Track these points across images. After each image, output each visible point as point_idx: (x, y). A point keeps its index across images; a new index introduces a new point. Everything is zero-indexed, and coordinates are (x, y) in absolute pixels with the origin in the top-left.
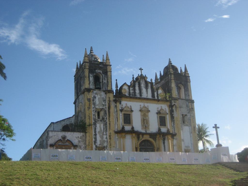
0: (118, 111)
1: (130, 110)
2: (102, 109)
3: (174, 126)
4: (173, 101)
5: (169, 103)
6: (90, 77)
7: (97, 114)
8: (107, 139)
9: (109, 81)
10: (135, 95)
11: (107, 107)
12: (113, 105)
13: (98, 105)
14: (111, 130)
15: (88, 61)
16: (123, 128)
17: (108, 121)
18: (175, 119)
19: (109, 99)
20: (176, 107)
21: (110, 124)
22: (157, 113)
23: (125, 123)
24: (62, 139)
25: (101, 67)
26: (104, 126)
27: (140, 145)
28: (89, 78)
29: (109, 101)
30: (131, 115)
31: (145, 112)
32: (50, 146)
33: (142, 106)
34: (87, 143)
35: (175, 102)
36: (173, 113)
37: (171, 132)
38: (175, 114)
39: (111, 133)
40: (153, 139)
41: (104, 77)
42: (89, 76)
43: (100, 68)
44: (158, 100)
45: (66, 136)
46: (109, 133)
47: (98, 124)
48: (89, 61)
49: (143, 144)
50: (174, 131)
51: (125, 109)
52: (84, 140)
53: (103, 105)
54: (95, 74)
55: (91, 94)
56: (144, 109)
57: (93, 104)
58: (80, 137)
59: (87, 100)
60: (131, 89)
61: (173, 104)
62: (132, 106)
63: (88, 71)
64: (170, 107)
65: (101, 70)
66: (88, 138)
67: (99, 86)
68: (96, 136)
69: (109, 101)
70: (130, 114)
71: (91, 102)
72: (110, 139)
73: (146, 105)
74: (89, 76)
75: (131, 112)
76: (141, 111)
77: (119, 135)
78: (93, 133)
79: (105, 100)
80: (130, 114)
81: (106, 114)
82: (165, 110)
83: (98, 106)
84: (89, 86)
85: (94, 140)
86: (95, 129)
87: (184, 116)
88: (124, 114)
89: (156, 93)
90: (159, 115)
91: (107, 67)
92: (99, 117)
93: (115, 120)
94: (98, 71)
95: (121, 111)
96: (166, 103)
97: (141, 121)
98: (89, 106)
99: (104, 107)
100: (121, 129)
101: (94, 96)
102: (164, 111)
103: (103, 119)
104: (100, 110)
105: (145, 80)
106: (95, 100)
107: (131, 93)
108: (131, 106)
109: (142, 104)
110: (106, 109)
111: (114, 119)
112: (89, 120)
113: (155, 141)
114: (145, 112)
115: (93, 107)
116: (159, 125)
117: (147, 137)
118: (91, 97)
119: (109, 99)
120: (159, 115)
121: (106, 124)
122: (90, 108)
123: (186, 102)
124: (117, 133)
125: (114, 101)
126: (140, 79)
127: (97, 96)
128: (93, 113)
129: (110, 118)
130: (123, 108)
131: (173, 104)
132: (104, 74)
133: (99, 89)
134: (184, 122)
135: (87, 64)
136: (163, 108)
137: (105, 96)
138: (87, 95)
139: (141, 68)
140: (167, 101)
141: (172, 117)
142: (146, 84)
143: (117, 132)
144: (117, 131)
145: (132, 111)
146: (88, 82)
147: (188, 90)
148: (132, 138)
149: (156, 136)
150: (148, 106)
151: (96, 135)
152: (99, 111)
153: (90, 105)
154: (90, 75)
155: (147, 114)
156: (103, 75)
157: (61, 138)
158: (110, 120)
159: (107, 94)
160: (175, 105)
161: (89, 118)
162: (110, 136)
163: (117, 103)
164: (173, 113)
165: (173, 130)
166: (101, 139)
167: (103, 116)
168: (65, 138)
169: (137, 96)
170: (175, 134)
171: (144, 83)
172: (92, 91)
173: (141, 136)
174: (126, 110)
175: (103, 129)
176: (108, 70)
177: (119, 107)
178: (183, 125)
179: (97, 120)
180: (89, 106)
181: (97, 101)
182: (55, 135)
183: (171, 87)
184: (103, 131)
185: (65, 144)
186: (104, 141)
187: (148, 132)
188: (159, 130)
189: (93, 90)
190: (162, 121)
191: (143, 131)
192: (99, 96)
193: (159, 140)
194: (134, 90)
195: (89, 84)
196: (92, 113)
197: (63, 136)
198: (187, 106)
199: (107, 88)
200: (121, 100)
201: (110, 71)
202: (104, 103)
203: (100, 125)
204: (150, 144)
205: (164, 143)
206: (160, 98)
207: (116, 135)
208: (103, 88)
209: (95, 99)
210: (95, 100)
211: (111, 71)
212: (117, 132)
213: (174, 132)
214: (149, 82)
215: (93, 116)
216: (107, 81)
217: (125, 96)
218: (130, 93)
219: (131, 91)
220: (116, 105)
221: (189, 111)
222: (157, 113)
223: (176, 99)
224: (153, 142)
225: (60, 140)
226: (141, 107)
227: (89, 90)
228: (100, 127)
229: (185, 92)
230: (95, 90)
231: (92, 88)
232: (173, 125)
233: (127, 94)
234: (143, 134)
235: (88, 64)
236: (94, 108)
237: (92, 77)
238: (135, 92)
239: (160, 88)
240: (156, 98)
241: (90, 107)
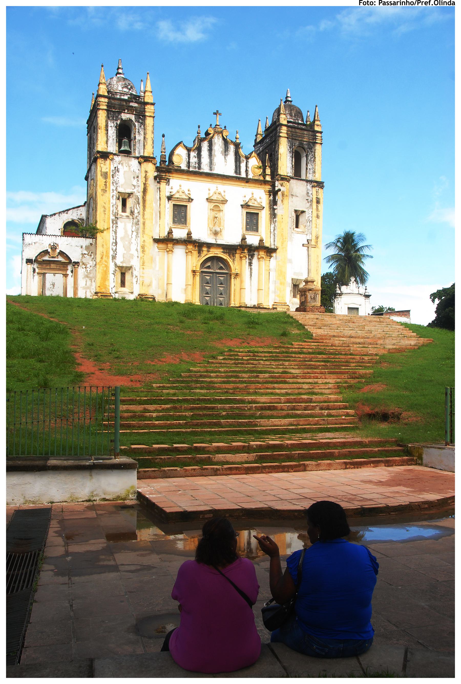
0: (161, 198)
1: (188, 198)
2: (130, 195)
3: (274, 234)
4: (277, 183)
5: (268, 188)
6: (110, 129)
7: (120, 204)
8: (138, 252)
9: (147, 137)
10: (199, 168)
11: (141, 189)
12: (152, 185)
13: (122, 185)
14: (145, 236)
15: (106, 94)
16: (170, 232)
17: (140, 217)
18: (278, 218)
19: (146, 175)
20: (283, 195)
21: (144, 224)
22: (242, 206)
23: (174, 222)
25: (132, 107)
26: (132, 227)
27: (203, 264)
28: (107, 130)
29: (146, 178)
30: (188, 207)
32: (27, 263)
33: (212, 193)
34: (98, 260)
35: (282, 185)
36: (275, 207)
37: (267, 244)
38: (280, 209)
39: (146, 241)
40: (229, 256)
41: (138, 129)
42: (107, 126)
43: (131, 110)
44: (247, 180)
45: (58, 245)
46: (142, 241)
47: (121, 222)
48: (108, 92)
49: (209, 264)
50: (272, 243)
51: (177, 196)
52: (92, 253)
53: (133, 185)
54: (119, 122)
55: (110, 164)
56: (214, 198)
57: (113, 183)
58: (84, 247)
59: (101, 175)
60: (193, 154)
61: (276, 189)
63: (106, 115)
64: (270, 195)
65: (133, 114)
66: (100, 250)
67: (127, 148)
68: (116, 245)
69: (146, 177)
70: (186, 206)
71: (107, 180)
72: (143, 251)
74: (107, 126)
75: (189, 202)
76: (209, 200)
77: (162, 246)
78: (112, 241)
79: (138, 177)
80: (186, 206)
81: (139, 204)
82: (259, 200)
83: (121, 187)
84: (106, 147)
85: (111, 253)
86: (116, 233)
87: (299, 212)
88: (174, 205)
89: (243, 165)
90: (245, 211)
91: (146, 107)
92: (124, 210)
93: (156, 215)
94: (125, 116)
95: (169, 198)
96: (263, 186)
97: (208, 221)
98: (104, 188)
99: (135, 190)
100: (166, 234)
101: (115, 168)
102: (256, 203)
103: (132, 213)
104: (128, 195)
105: (222, 136)
106: (118, 176)
107: (192, 163)
110: (138, 194)
111: (153, 214)
112: (103, 215)
113: (234, 260)
115: (113, 190)
116: (244, 229)
117: (218, 253)
118: (110, 170)
119: (146, 175)
120: (245, 211)
121: (137, 224)
122: (106, 191)
123: (307, 185)
124: (157, 242)
125: (155, 178)
126: (211, 135)
127: (122, 167)
128: (111, 202)
129: (145, 213)
130: (172, 194)
131: (276, 189)
132: (138, 122)
133: (127, 153)
134: (297, 226)
135: (102, 99)
136: (256, 196)
137: (139, 168)
138: (102, 165)
139: (217, 111)
140: (265, 182)
141: (273, 215)
142: (225, 148)
143: (157, 241)
144: (159, 238)
145: (190, 200)
146: (105, 139)
147: (314, 161)
148: (186, 253)
149: (236, 251)
150: (224, 192)
151: (116, 243)
152: (126, 197)
153: (106, 185)
154: (109, 123)
156: (136, 124)
157: (48, 248)
158: (145, 217)
159: (142, 165)
160: (279, 190)
161: (105, 211)
162: (143, 247)
163: (161, 183)
164: (275, 207)
165: (272, 240)
166: (125, 252)
167: (131, 207)
168: (56, 248)
169: (204, 169)
170: (276, 248)
171: (221, 144)
172: (111, 157)
173: (205, 249)
174: (178, 197)
175: (130, 233)
176: (147, 114)
177: (166, 189)
178: (295, 232)
179: (121, 215)
180: (104, 188)
181: (121, 177)
182: (37, 242)
183: (278, 154)
184: (130, 237)
185: (56, 259)
186: (132, 256)
187: (219, 242)
188: (244, 239)
189: (115, 154)
191: (211, 240)
192: (126, 169)
193: (241, 257)
194: (199, 156)
195: (107, 142)
196: (110, 201)
197: (52, 244)
198: (308, 193)
199: (144, 152)
200: (170, 178)
201: (150, 116)
202: (135, 182)
203: (125, 225)
204: (222, 265)
205: (250, 264)
206: (250, 176)
207: (156, 245)
208: (134, 152)
209: (117, 173)
210: (118, 176)
211: (154, 117)
212: (157, 241)
213: (274, 245)
214: (232, 142)
215: (113, 206)
216: (145, 138)
217: (179, 171)
218: (189, 163)
219: (191, 159)
220: (160, 188)
221: (310, 203)
222: (242, 206)
223: (285, 179)
224: (229, 261)
225: (46, 252)
226: (209, 194)
227: (105, 155)
228: (125, 229)
229: (307, 165)
230: (118, 155)
231: (111, 151)
232: (272, 231)
233: (184, 167)
234: (209, 246)
235: (106, 100)
236: (115, 191)
237: (114, 128)
238: (199, 163)
239: (254, 154)
240: (243, 175)
241: (107, 189)
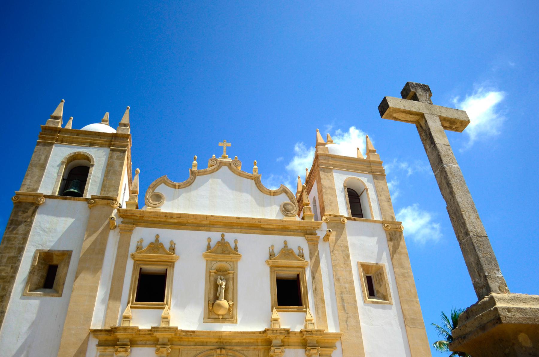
33: (213, 244)
62: (175, 242)
73: (230, 237)
108: (171, 242)
109: (215, 236)
150: (236, 241)
226: (209, 247)
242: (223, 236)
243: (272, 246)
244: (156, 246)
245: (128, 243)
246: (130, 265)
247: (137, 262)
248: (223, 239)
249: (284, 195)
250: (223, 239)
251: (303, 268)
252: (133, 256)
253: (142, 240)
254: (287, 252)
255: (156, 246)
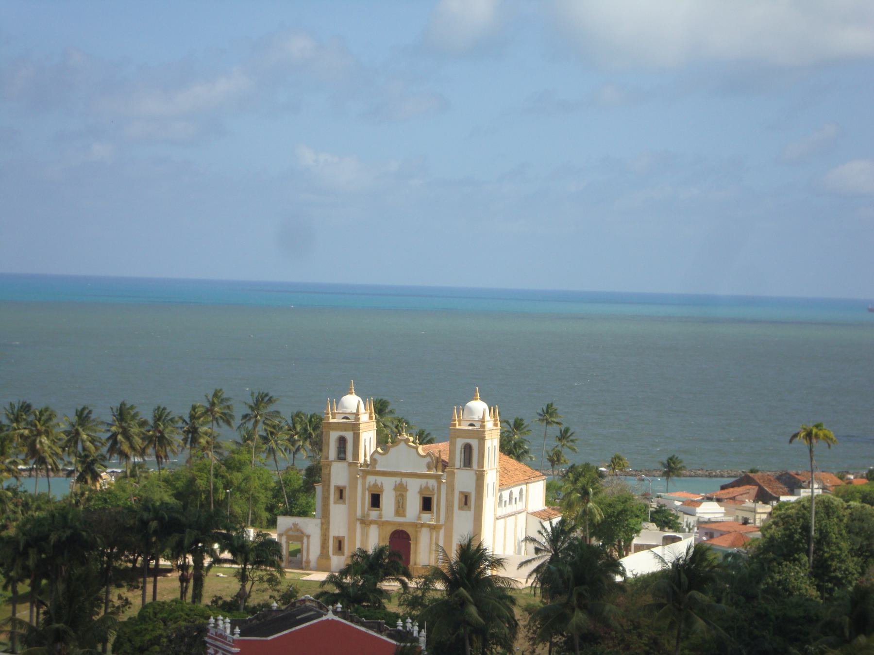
24: (293, 527)
31: (401, 492)
33: (397, 483)
73: (405, 480)
108: (381, 483)
109: (398, 479)
114: (401, 492)
133: (344, 459)
150: (407, 483)
155: (404, 493)
190: (427, 504)
225: (290, 529)
242: (401, 479)
243: (421, 486)
244: (375, 485)
245: (366, 482)
246: (367, 493)
247: (369, 491)
248: (401, 482)
249: (429, 457)
250: (401, 482)
251: (433, 495)
252: (367, 489)
253: (370, 483)
254: (427, 488)
255: (375, 485)
